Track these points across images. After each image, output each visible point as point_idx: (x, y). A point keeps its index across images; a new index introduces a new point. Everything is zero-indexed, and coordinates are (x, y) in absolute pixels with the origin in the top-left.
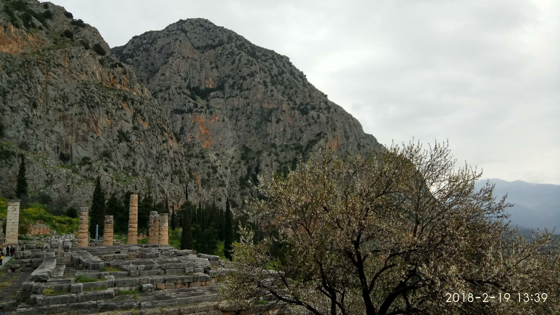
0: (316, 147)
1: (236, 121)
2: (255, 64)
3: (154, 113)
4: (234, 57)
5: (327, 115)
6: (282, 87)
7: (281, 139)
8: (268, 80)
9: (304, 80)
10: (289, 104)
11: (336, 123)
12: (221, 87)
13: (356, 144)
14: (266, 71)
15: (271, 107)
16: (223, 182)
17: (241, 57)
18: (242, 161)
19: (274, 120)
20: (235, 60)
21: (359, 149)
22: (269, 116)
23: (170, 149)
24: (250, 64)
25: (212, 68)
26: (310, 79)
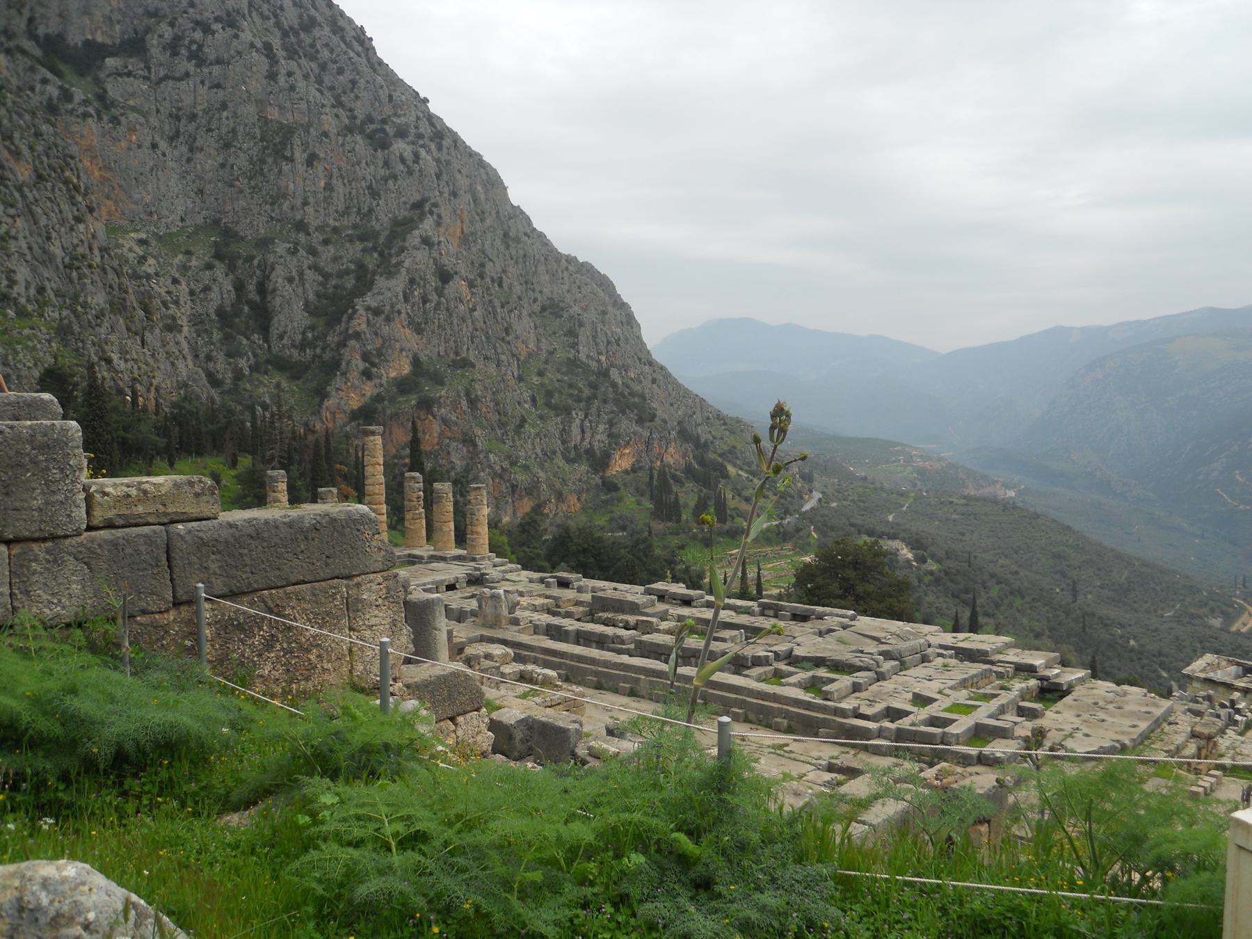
0: (414, 238)
1: (191, 150)
3: (38, 134)
6: (313, 65)
7: (322, 210)
8: (276, 43)
9: (367, 50)
10: (337, 116)
11: (458, 176)
12: (135, 46)
13: (500, 232)
14: (267, 13)
15: (288, 119)
16: (174, 318)
18: (217, 263)
19: (300, 156)
21: (508, 247)
22: (284, 144)
26: (385, 50)
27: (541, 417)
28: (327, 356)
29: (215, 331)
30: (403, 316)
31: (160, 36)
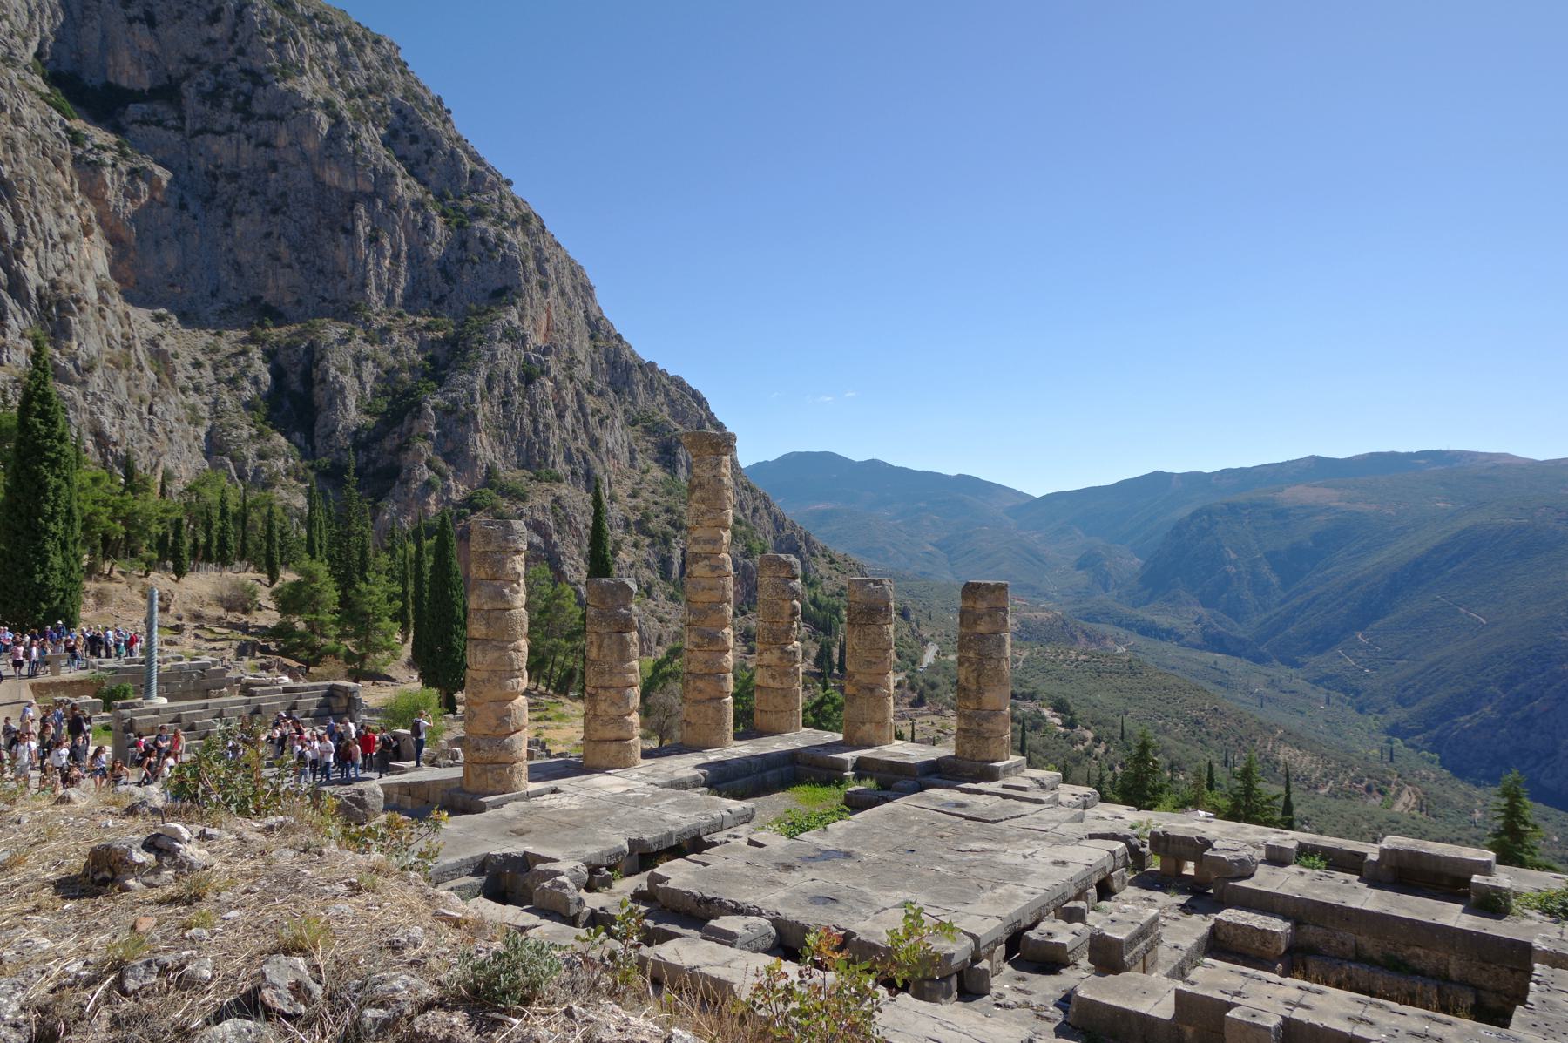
1: (229, 214)
5: (521, 236)
10: (408, 187)
11: (547, 266)
15: (350, 186)
16: (193, 408)
19: (363, 229)
20: (220, 10)
23: (85, 271)
25: (131, 21)
27: (635, 545)
28: (381, 464)
30: (480, 417)
31: (199, 84)
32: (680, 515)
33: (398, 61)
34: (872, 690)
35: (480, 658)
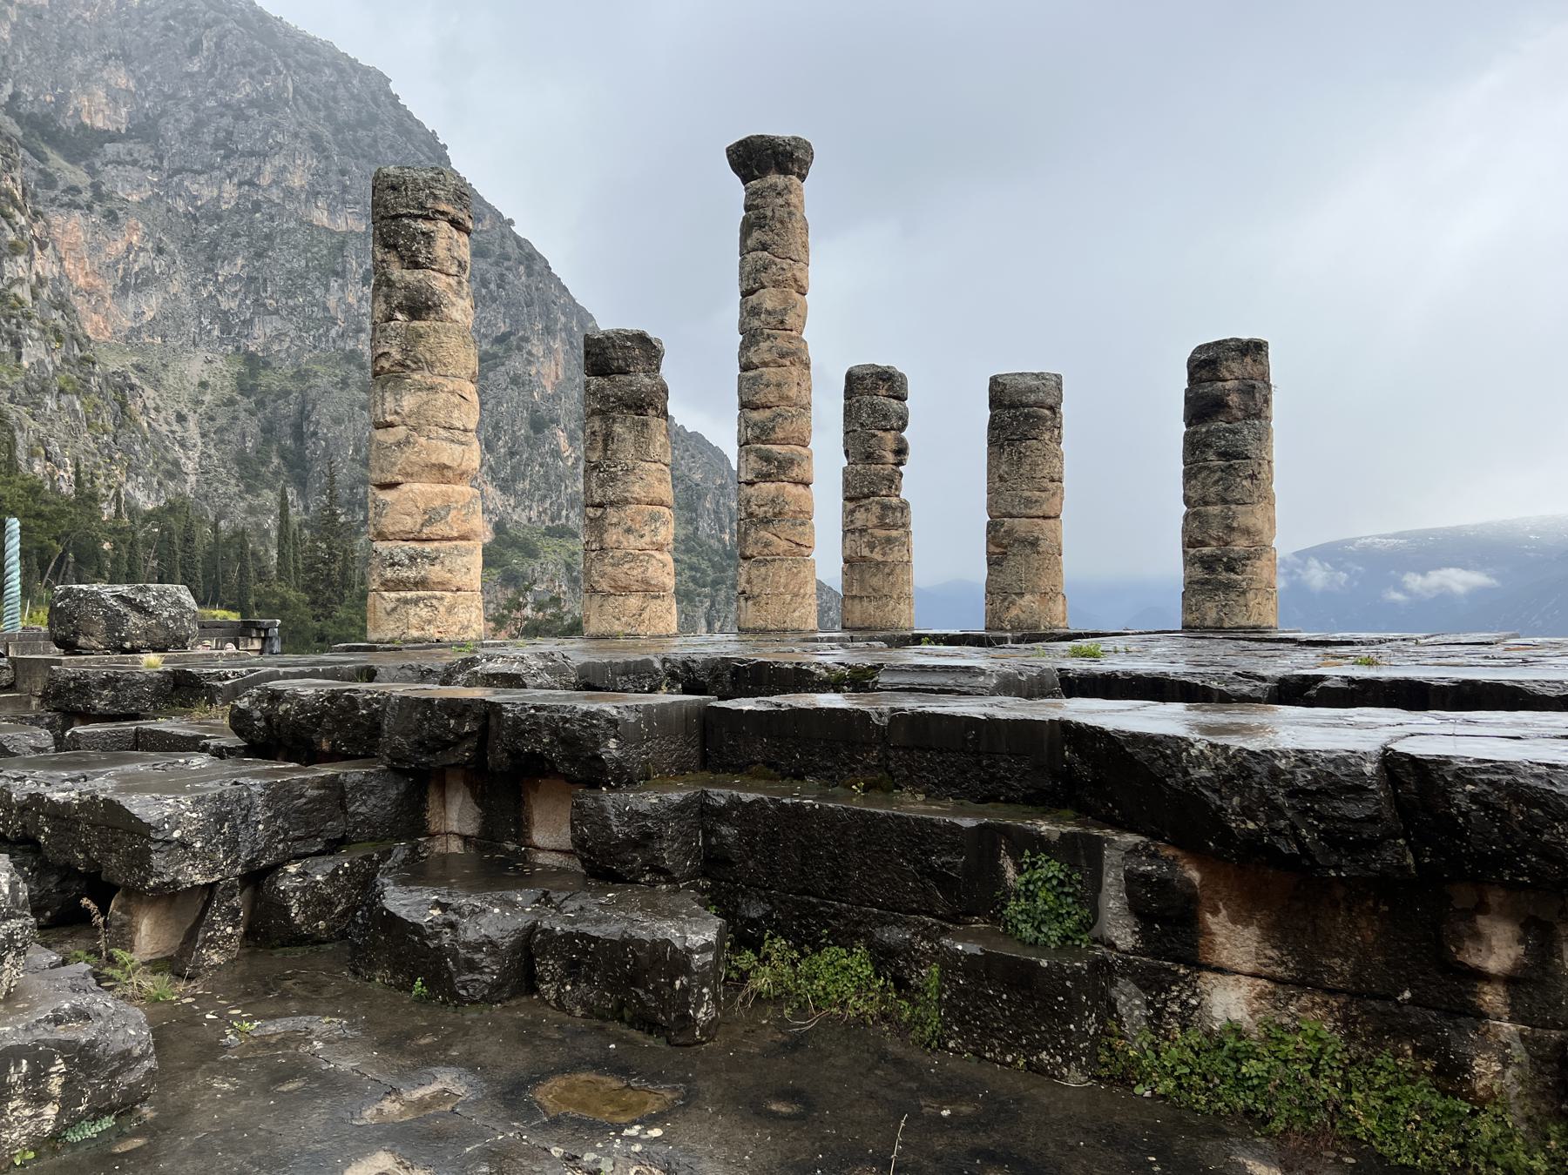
2: (279, 73)
4: (194, 31)
15: (341, 225)
16: (176, 463)
17: (222, 37)
24: (260, 65)
29: (233, 481)
32: (704, 572)
33: (389, 94)
34: (1034, 544)
35: (390, 404)
